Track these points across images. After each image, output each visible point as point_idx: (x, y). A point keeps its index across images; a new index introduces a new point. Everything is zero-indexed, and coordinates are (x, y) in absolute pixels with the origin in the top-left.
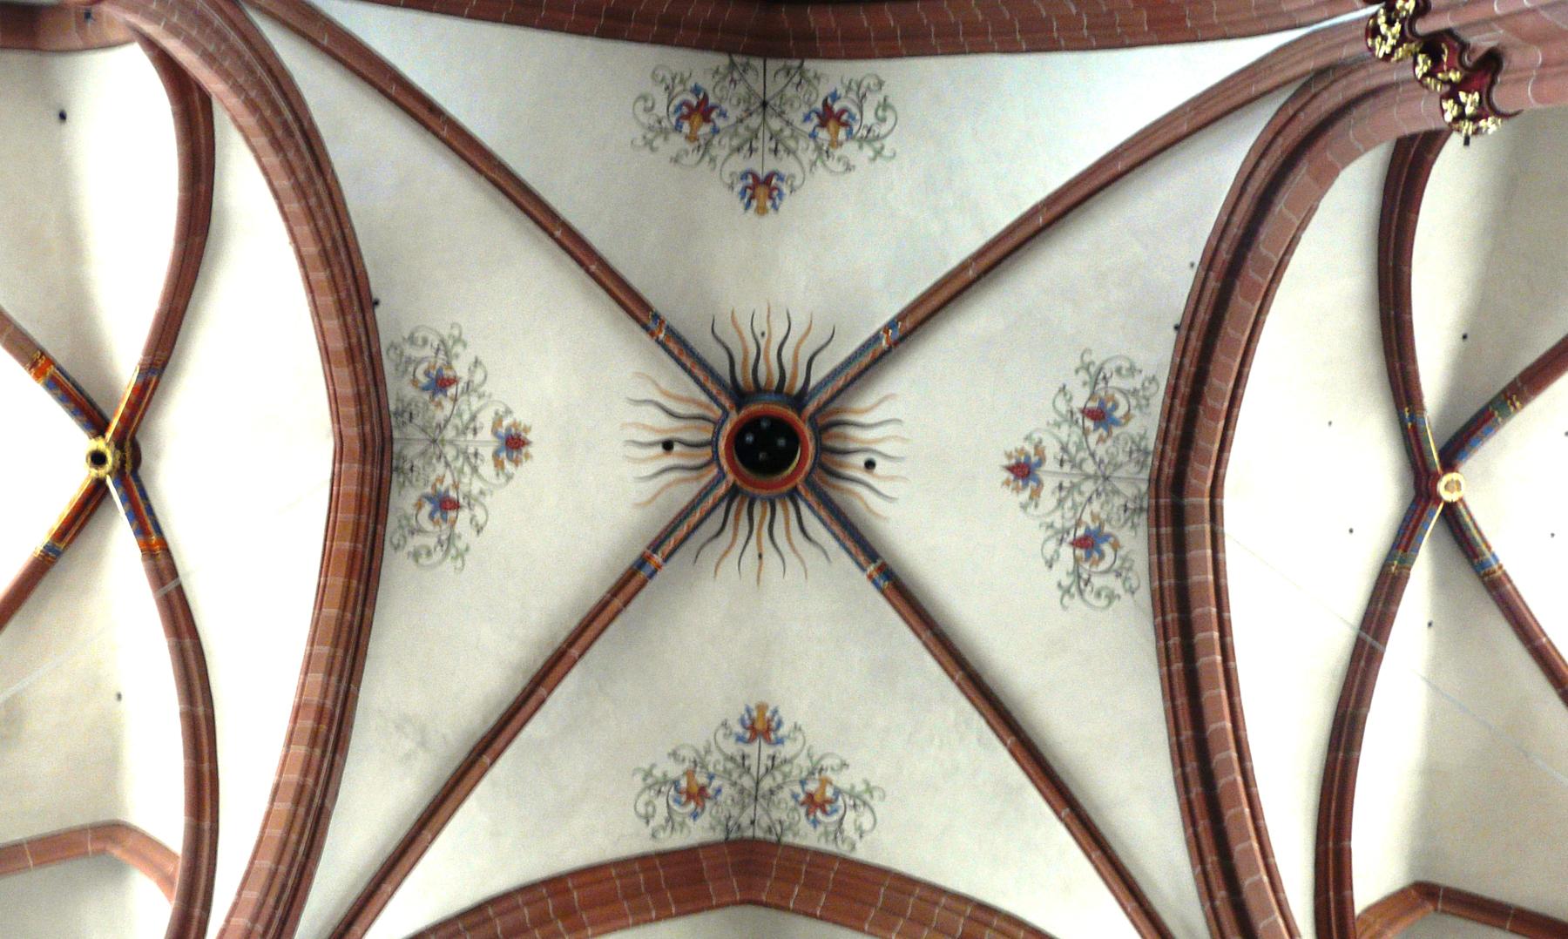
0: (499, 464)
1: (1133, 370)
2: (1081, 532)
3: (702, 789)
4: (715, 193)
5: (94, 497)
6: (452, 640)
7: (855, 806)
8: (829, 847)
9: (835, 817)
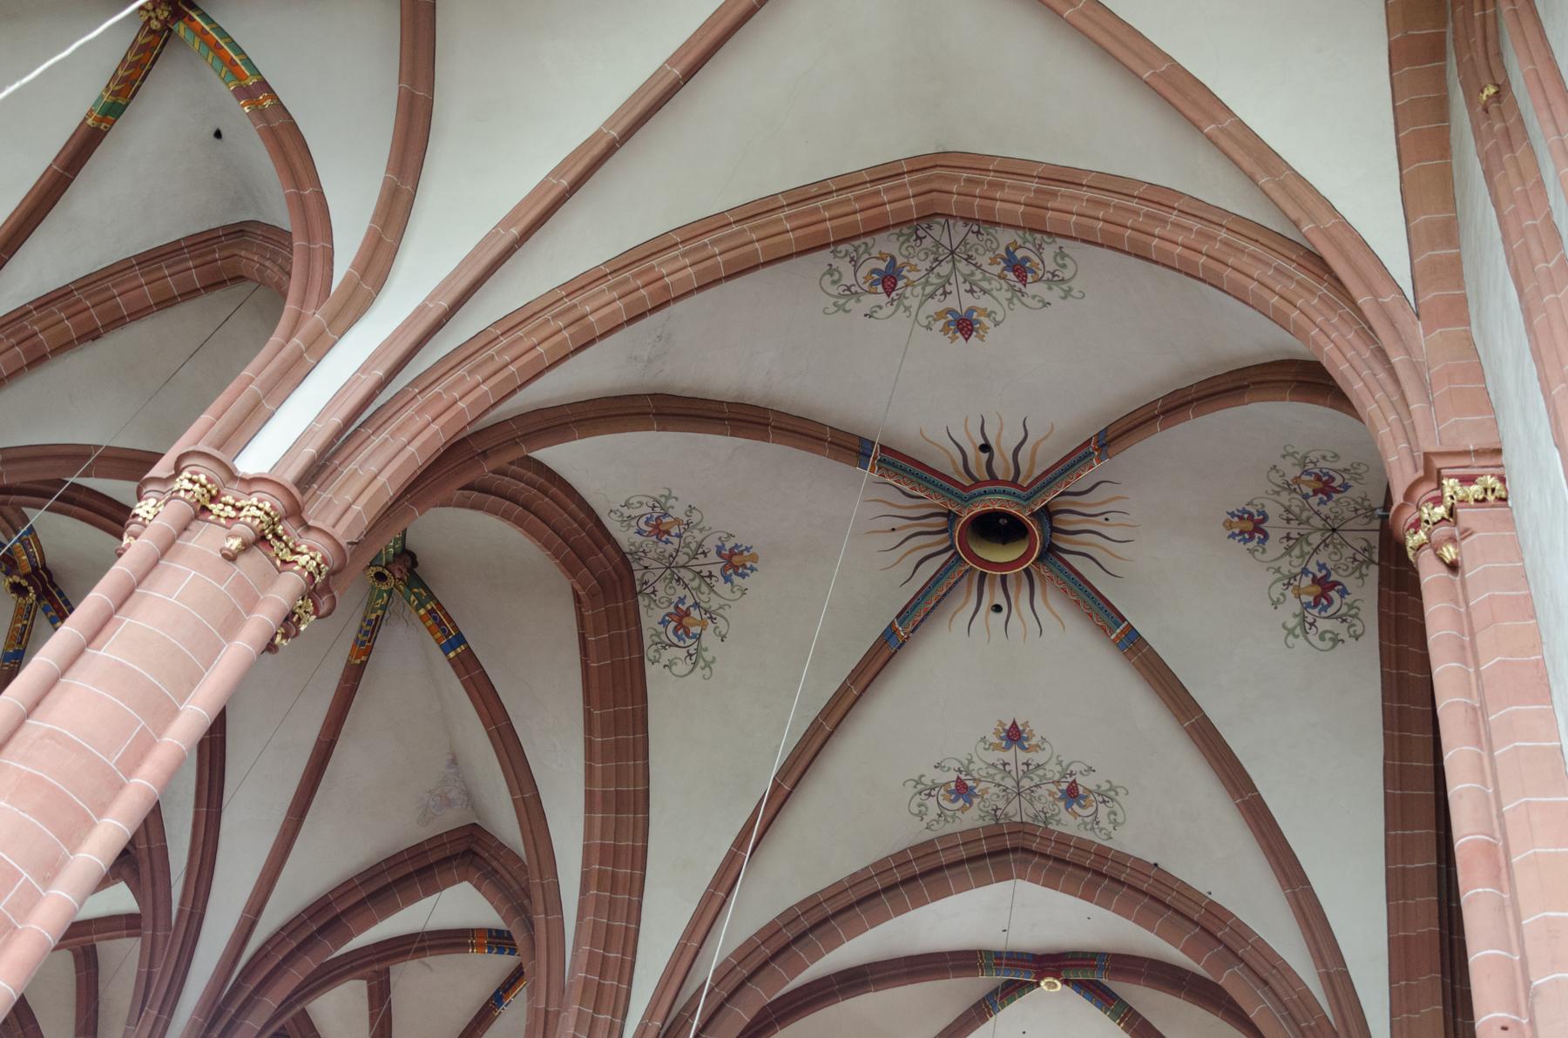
0: (939, 315)
1: (1115, 824)
2: (970, 783)
3: (668, 533)
7: (690, 655)
8: (647, 642)
9: (675, 640)
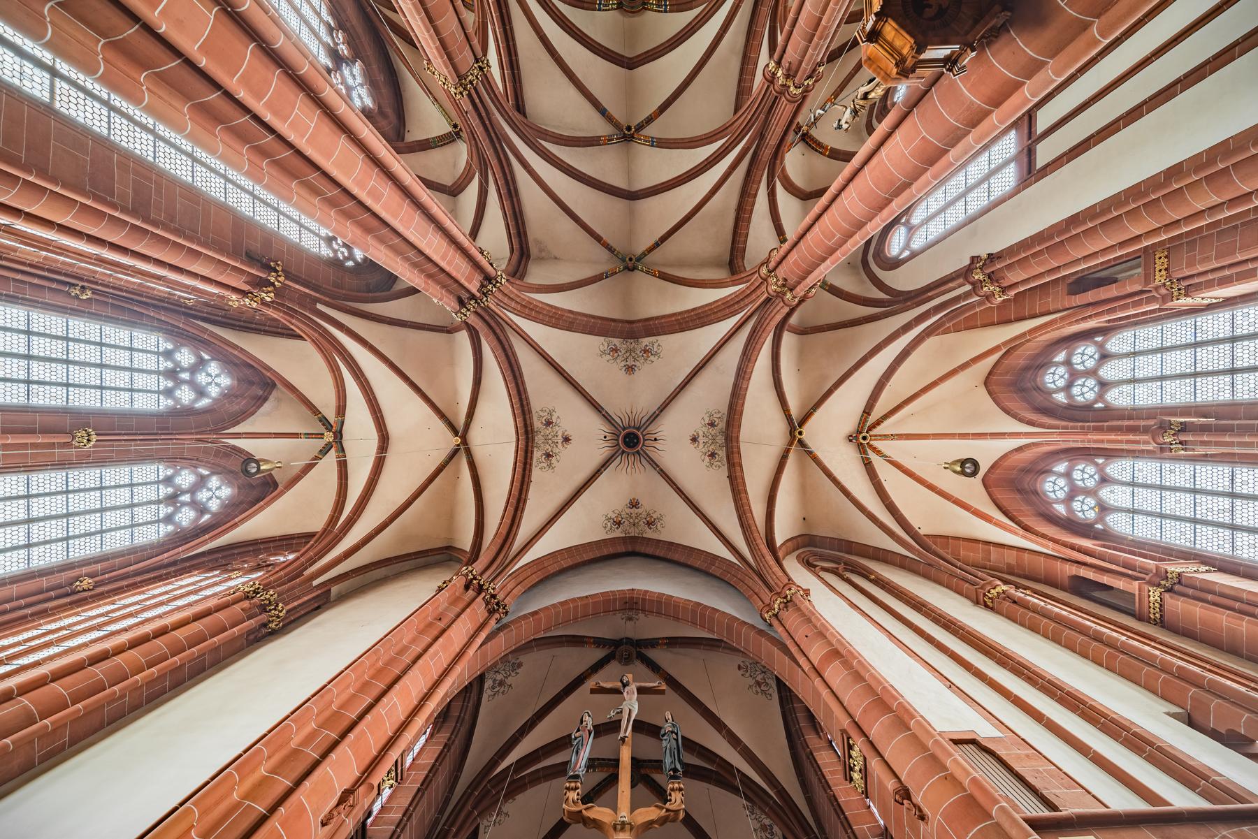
4: (646, 504)
5: (802, 423)
6: (709, 394)
